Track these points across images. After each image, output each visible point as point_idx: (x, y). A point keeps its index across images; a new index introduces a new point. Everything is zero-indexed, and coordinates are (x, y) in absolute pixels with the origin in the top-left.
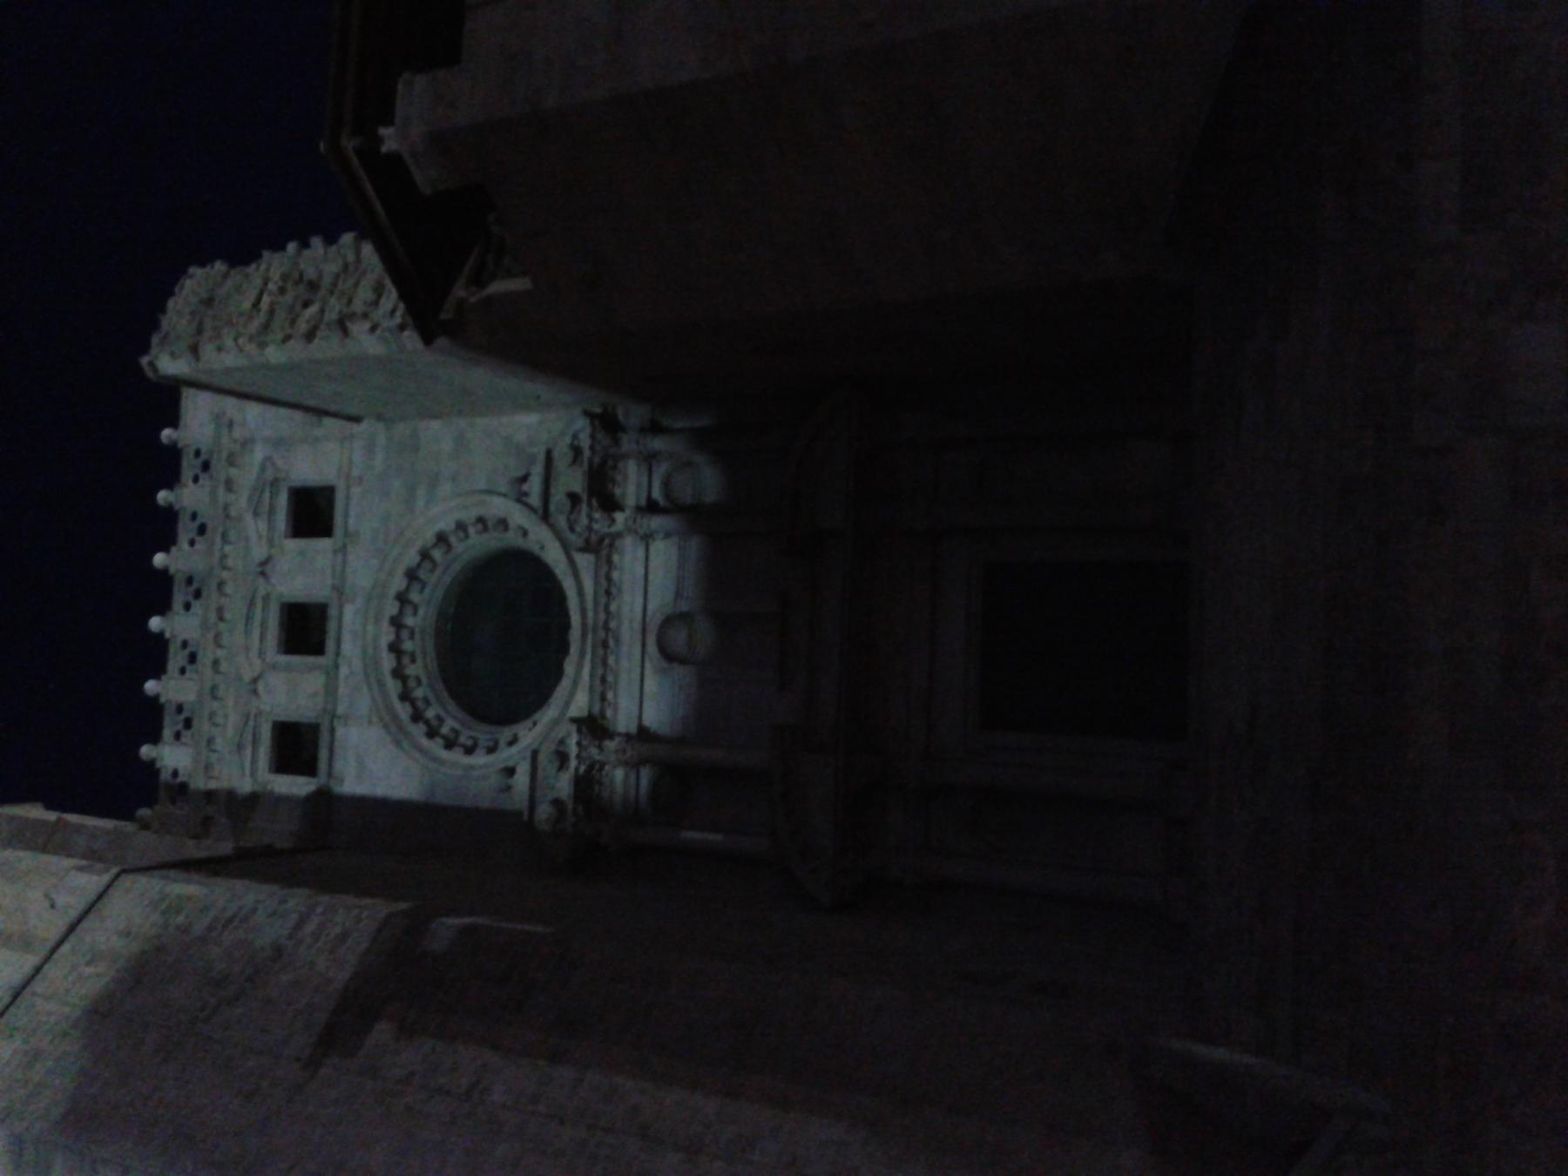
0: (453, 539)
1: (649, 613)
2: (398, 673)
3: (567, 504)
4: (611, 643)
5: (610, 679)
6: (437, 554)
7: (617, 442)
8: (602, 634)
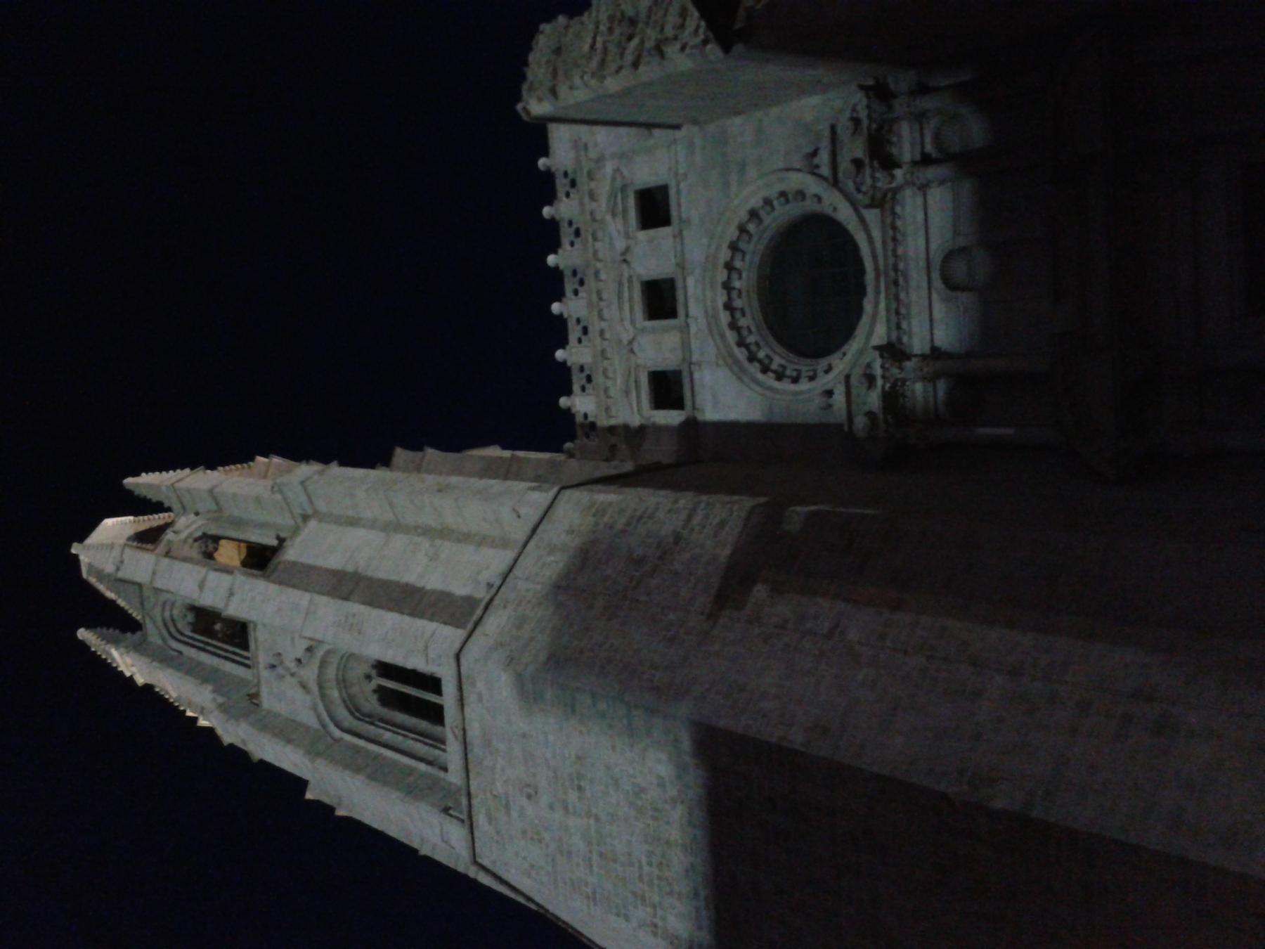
0: (762, 213)
1: (932, 253)
2: (733, 326)
3: (852, 169)
4: (901, 281)
5: (903, 311)
6: (751, 227)
7: (890, 108)
8: (892, 274)
